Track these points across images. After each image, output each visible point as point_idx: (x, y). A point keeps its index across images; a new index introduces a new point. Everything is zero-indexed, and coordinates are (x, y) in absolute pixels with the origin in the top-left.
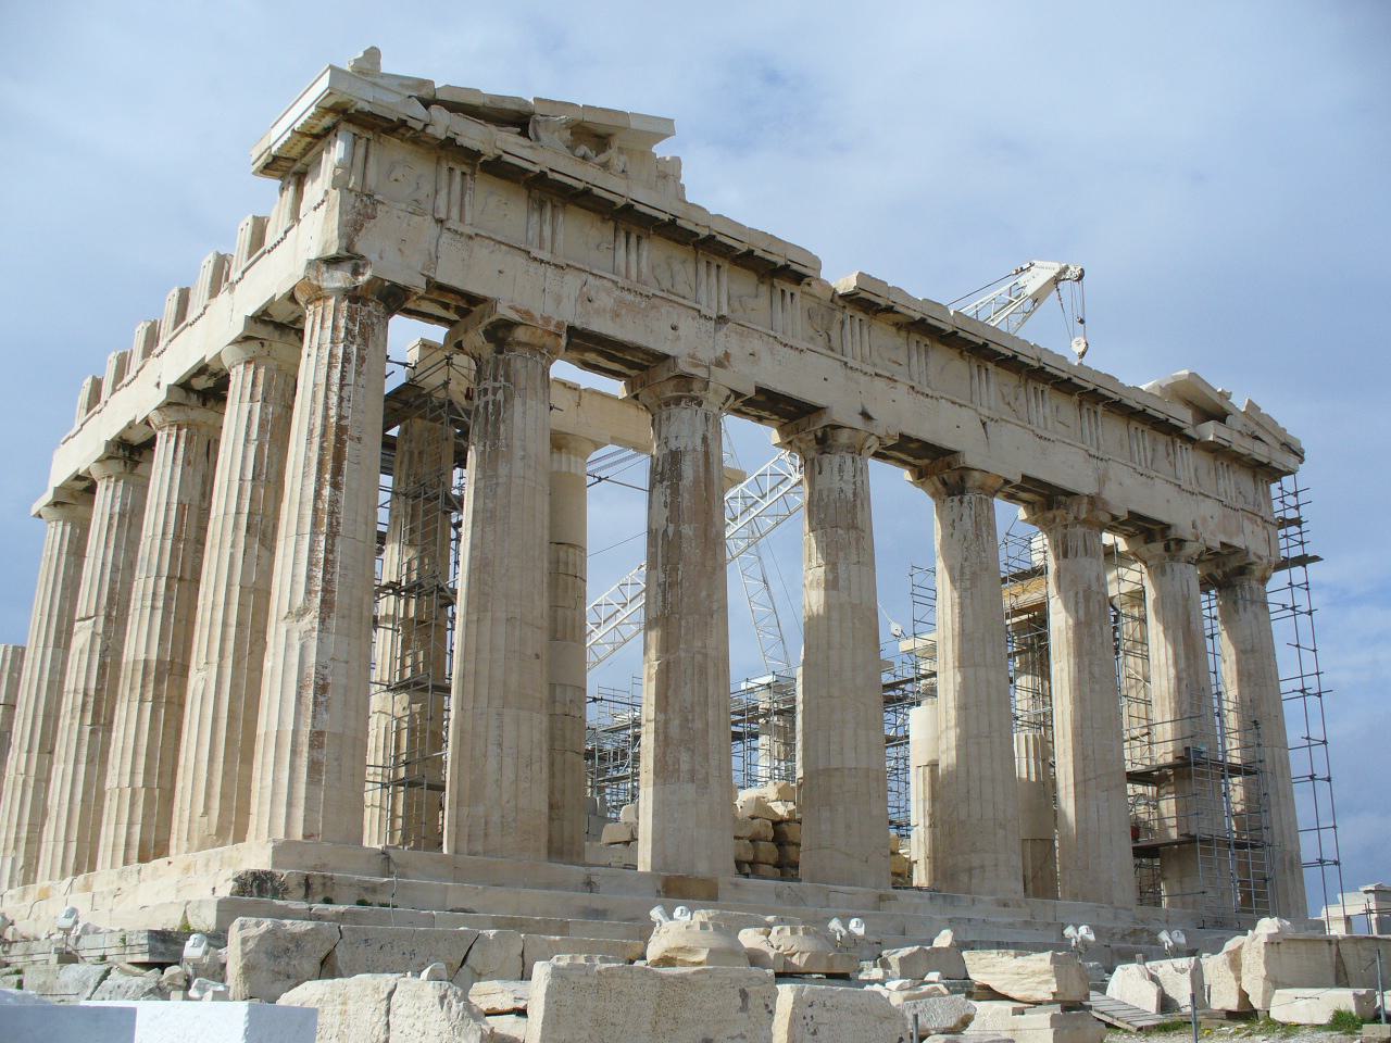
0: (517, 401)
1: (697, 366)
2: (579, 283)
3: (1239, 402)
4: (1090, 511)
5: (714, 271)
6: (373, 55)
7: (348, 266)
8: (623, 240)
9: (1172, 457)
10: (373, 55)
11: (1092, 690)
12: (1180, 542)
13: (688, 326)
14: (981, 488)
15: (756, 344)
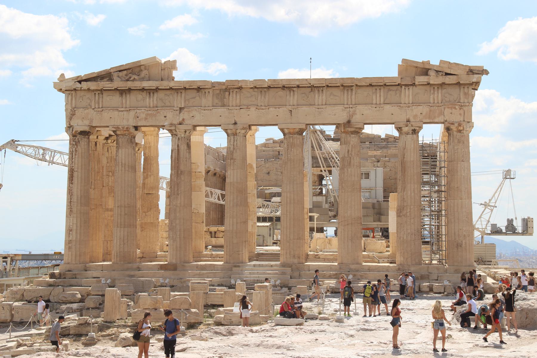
0: (120, 150)
1: (171, 127)
2: (134, 113)
3: (435, 62)
4: (344, 128)
5: (179, 94)
6: (62, 75)
7: (71, 129)
8: (148, 96)
9: (398, 95)
10: (62, 75)
11: (342, 192)
12: (400, 128)
13: (170, 115)
14: (290, 133)
15: (194, 113)
